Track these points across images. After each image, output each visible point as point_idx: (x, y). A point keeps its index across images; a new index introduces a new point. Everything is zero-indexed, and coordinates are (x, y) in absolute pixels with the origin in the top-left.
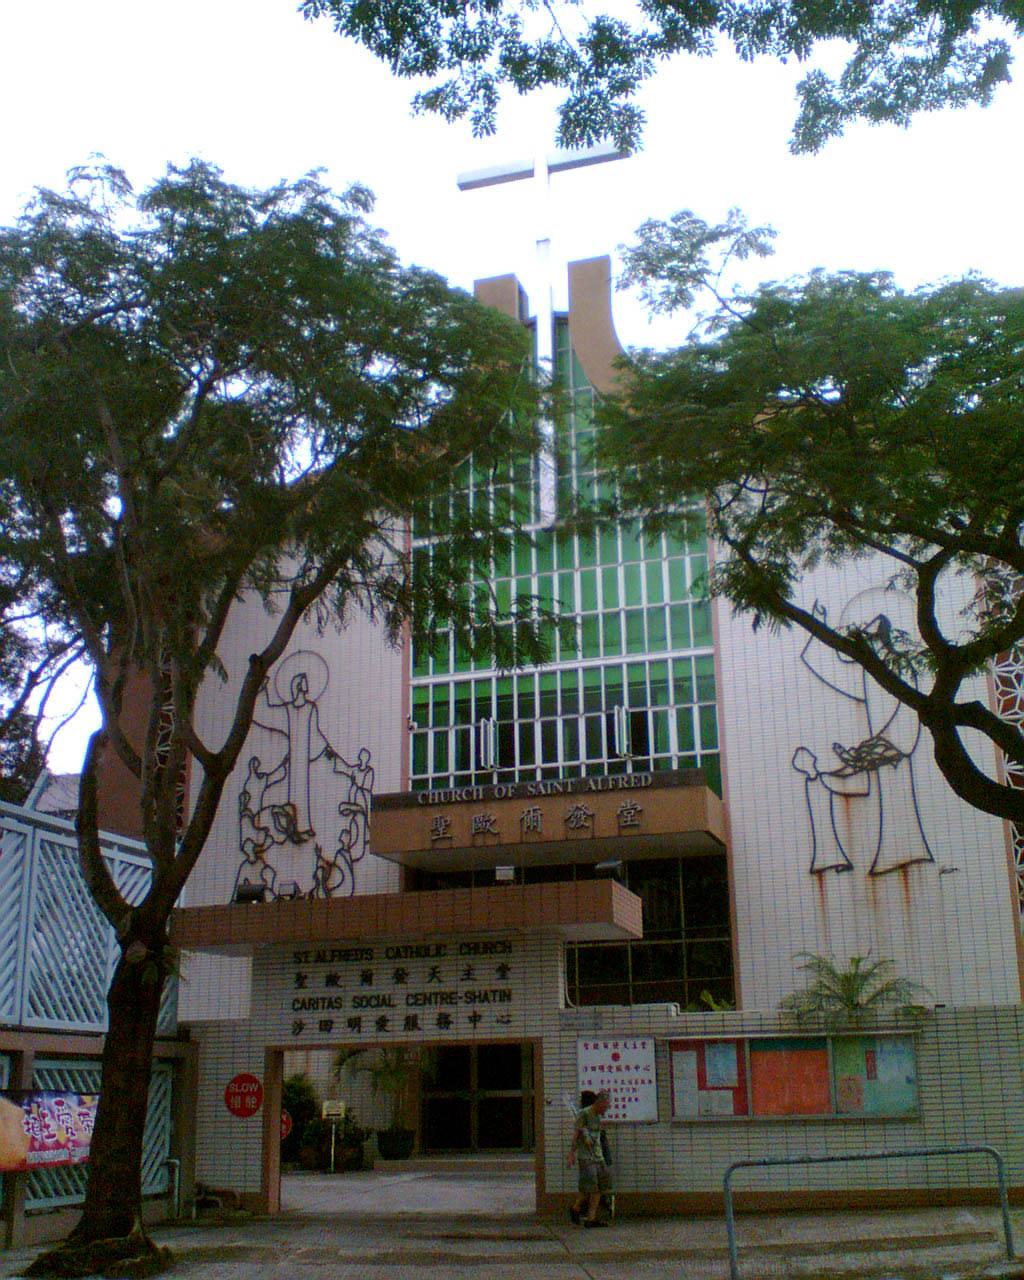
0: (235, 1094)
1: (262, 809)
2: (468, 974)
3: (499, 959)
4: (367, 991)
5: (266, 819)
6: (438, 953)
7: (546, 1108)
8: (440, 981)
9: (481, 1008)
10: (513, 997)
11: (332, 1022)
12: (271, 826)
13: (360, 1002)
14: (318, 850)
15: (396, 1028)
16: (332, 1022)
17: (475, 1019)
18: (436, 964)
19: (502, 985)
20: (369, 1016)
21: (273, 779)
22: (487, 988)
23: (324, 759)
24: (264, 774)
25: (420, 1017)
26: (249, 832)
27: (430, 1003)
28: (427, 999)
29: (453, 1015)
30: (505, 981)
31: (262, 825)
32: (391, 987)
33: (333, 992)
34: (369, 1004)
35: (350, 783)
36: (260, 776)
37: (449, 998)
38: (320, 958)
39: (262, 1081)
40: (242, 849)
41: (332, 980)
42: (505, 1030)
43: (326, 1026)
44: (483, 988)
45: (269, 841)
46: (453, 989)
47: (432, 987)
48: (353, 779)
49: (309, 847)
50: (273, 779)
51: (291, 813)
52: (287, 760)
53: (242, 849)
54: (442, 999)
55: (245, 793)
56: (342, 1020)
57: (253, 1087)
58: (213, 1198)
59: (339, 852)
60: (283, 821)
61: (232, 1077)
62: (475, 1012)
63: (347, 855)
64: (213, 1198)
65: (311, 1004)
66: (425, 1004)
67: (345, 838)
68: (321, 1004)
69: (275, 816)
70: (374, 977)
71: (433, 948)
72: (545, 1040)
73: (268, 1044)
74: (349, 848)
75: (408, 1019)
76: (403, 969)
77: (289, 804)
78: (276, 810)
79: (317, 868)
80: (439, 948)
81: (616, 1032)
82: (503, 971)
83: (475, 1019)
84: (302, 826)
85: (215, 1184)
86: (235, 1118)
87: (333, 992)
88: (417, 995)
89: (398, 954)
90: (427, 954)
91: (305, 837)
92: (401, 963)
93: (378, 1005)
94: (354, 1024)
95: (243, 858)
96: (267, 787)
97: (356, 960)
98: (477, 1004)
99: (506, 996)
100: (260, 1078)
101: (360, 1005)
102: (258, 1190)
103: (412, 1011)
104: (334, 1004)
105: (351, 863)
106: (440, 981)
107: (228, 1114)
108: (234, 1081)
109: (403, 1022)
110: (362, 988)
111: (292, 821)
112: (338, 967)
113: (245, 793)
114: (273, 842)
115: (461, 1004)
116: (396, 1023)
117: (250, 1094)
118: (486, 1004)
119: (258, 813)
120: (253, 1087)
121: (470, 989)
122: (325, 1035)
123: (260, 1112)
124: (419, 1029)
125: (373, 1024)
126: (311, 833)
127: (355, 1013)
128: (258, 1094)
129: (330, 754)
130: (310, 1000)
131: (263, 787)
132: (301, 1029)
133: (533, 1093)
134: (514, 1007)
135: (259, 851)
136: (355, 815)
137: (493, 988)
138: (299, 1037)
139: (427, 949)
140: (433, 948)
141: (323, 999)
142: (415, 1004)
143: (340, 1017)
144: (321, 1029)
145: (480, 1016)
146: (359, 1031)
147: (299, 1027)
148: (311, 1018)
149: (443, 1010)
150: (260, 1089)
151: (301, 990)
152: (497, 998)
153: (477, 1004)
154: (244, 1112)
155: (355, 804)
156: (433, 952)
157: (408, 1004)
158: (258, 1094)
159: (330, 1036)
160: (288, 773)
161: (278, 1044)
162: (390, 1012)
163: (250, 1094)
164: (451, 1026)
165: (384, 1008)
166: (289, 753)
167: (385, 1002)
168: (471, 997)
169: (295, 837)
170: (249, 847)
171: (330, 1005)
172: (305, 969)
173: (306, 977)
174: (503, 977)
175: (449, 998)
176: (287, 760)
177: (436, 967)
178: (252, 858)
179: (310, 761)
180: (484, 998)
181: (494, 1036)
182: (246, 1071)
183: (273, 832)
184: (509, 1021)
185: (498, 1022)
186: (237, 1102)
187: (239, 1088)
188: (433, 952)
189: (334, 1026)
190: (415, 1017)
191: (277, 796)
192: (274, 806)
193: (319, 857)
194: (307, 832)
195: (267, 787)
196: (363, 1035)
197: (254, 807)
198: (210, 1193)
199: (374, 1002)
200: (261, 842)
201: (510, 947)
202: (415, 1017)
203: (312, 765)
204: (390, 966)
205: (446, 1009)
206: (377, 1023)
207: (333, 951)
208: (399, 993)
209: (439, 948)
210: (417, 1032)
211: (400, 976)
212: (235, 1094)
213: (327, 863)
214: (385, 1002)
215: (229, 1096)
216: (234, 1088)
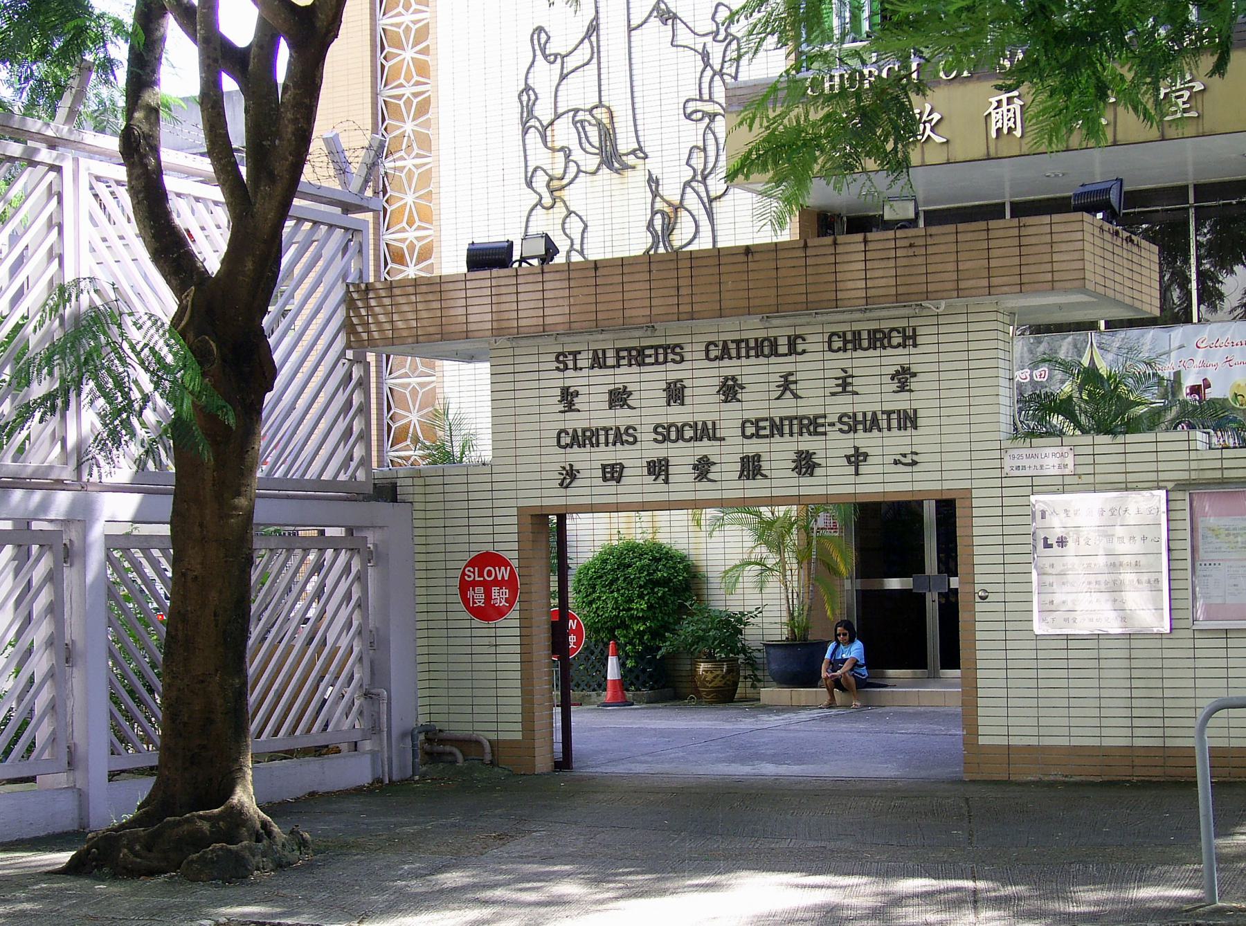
0: (474, 584)
1: (558, 116)
2: (845, 385)
3: (895, 358)
4: (677, 414)
5: (564, 133)
6: (792, 350)
7: (979, 607)
8: (796, 396)
9: (864, 440)
10: (920, 422)
11: (622, 467)
12: (574, 144)
13: (665, 433)
14: (653, 183)
15: (725, 476)
16: (622, 467)
17: (857, 459)
18: (790, 368)
19: (901, 402)
20: (682, 455)
21: (571, 63)
22: (877, 407)
23: (654, 22)
24: (556, 56)
25: (765, 457)
26: (539, 155)
27: (782, 435)
28: (777, 428)
29: (821, 454)
30: (905, 395)
31: (558, 145)
32: (716, 407)
33: (621, 417)
34: (680, 436)
35: (701, 65)
36: (551, 59)
37: (812, 425)
38: (598, 362)
39: (515, 563)
40: (529, 184)
41: (619, 398)
42: (908, 477)
43: (613, 473)
44: (869, 408)
45: (572, 169)
46: (820, 411)
47: (786, 408)
48: (705, 56)
49: (637, 179)
50: (571, 63)
51: (606, 121)
52: (594, 28)
53: (529, 184)
54: (801, 426)
55: (527, 88)
56: (638, 463)
57: (503, 573)
58: (448, 748)
59: (687, 184)
60: (593, 133)
61: (468, 557)
62: (856, 449)
63: (701, 189)
64: (448, 748)
65: (585, 438)
66: (772, 435)
67: (698, 161)
68: (602, 439)
69: (579, 125)
70: (687, 392)
71: (783, 341)
72: (975, 493)
73: (522, 503)
74: (705, 178)
75: (745, 461)
76: (733, 378)
77: (600, 105)
78: (580, 116)
79: (654, 213)
80: (792, 342)
81: (1099, 478)
82: (903, 378)
83: (857, 459)
84: (625, 143)
85: (453, 726)
86: (477, 622)
87: (621, 417)
88: (758, 420)
89: (725, 353)
90: (774, 352)
91: (631, 160)
92: (730, 368)
93: (695, 438)
94: (658, 469)
95: (535, 198)
96: (563, 77)
97: (657, 363)
98: (861, 434)
99: (908, 420)
100: (512, 556)
101: (666, 439)
102: (519, 736)
103: (753, 447)
104: (622, 436)
105: (709, 203)
106: (796, 396)
107: (468, 615)
108: (472, 563)
109: (738, 467)
110: (671, 410)
111: (608, 135)
112: (626, 376)
113: (527, 88)
114: (579, 171)
115: (833, 434)
116: (725, 467)
117: (496, 583)
118: (875, 433)
119: (551, 124)
120: (503, 573)
121: (848, 409)
122: (611, 487)
123: (514, 614)
124: (765, 477)
125: (690, 469)
126: (640, 152)
127: (659, 452)
128: (511, 583)
129: (668, 17)
130: (584, 431)
131: (556, 78)
132: (573, 478)
133: (954, 582)
134: (921, 440)
135: (556, 187)
136: (712, 120)
137: (887, 407)
138: (570, 491)
139: (774, 344)
140: (783, 341)
141: (606, 430)
142: (757, 435)
143: (633, 458)
144: (605, 479)
145: (866, 455)
146: (666, 481)
147: (570, 475)
148: (588, 460)
149: (803, 447)
150: (512, 572)
151: (569, 415)
152: (894, 423)
153: (861, 434)
154: (488, 613)
155: (711, 100)
156: (783, 349)
157: (744, 435)
158: (511, 583)
159: (621, 489)
160: (596, 52)
161: (537, 502)
162: (716, 450)
163: (496, 583)
164: (818, 471)
165: (705, 442)
166: (596, 18)
167: (706, 432)
168: (851, 423)
169: (610, 157)
170: (540, 181)
171: (619, 439)
172: (573, 380)
173: (577, 393)
174: (903, 388)
175: (812, 425)
176: (594, 28)
177: (791, 374)
178: (547, 201)
179: (630, 30)
180: (872, 423)
181: (890, 488)
182: (489, 548)
183: (577, 155)
184: (914, 463)
185: (896, 462)
186: (478, 596)
187: (481, 575)
188: (783, 349)
189: (626, 472)
190: (757, 457)
191: (579, 92)
192: (576, 111)
193: (655, 194)
194: (633, 152)
195: (563, 77)
196: (672, 487)
197: (544, 111)
198: (442, 741)
199: (689, 433)
200: (558, 172)
201: (914, 337)
202: (757, 457)
203: (633, 33)
204: (715, 372)
205: (807, 443)
206: (695, 467)
207: (618, 351)
208: (729, 418)
209: (792, 342)
210: (759, 482)
211: (730, 390)
212: (474, 584)
213: (669, 204)
214: (706, 432)
215: (465, 586)
216: (473, 576)
